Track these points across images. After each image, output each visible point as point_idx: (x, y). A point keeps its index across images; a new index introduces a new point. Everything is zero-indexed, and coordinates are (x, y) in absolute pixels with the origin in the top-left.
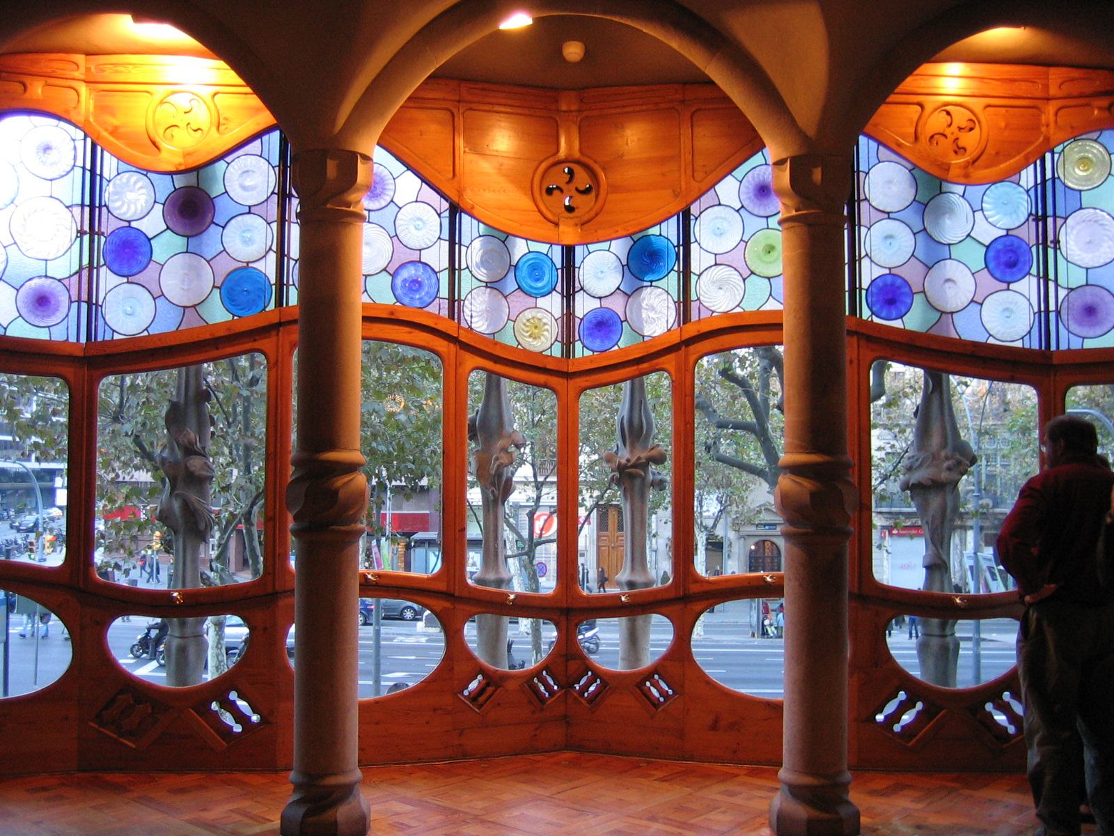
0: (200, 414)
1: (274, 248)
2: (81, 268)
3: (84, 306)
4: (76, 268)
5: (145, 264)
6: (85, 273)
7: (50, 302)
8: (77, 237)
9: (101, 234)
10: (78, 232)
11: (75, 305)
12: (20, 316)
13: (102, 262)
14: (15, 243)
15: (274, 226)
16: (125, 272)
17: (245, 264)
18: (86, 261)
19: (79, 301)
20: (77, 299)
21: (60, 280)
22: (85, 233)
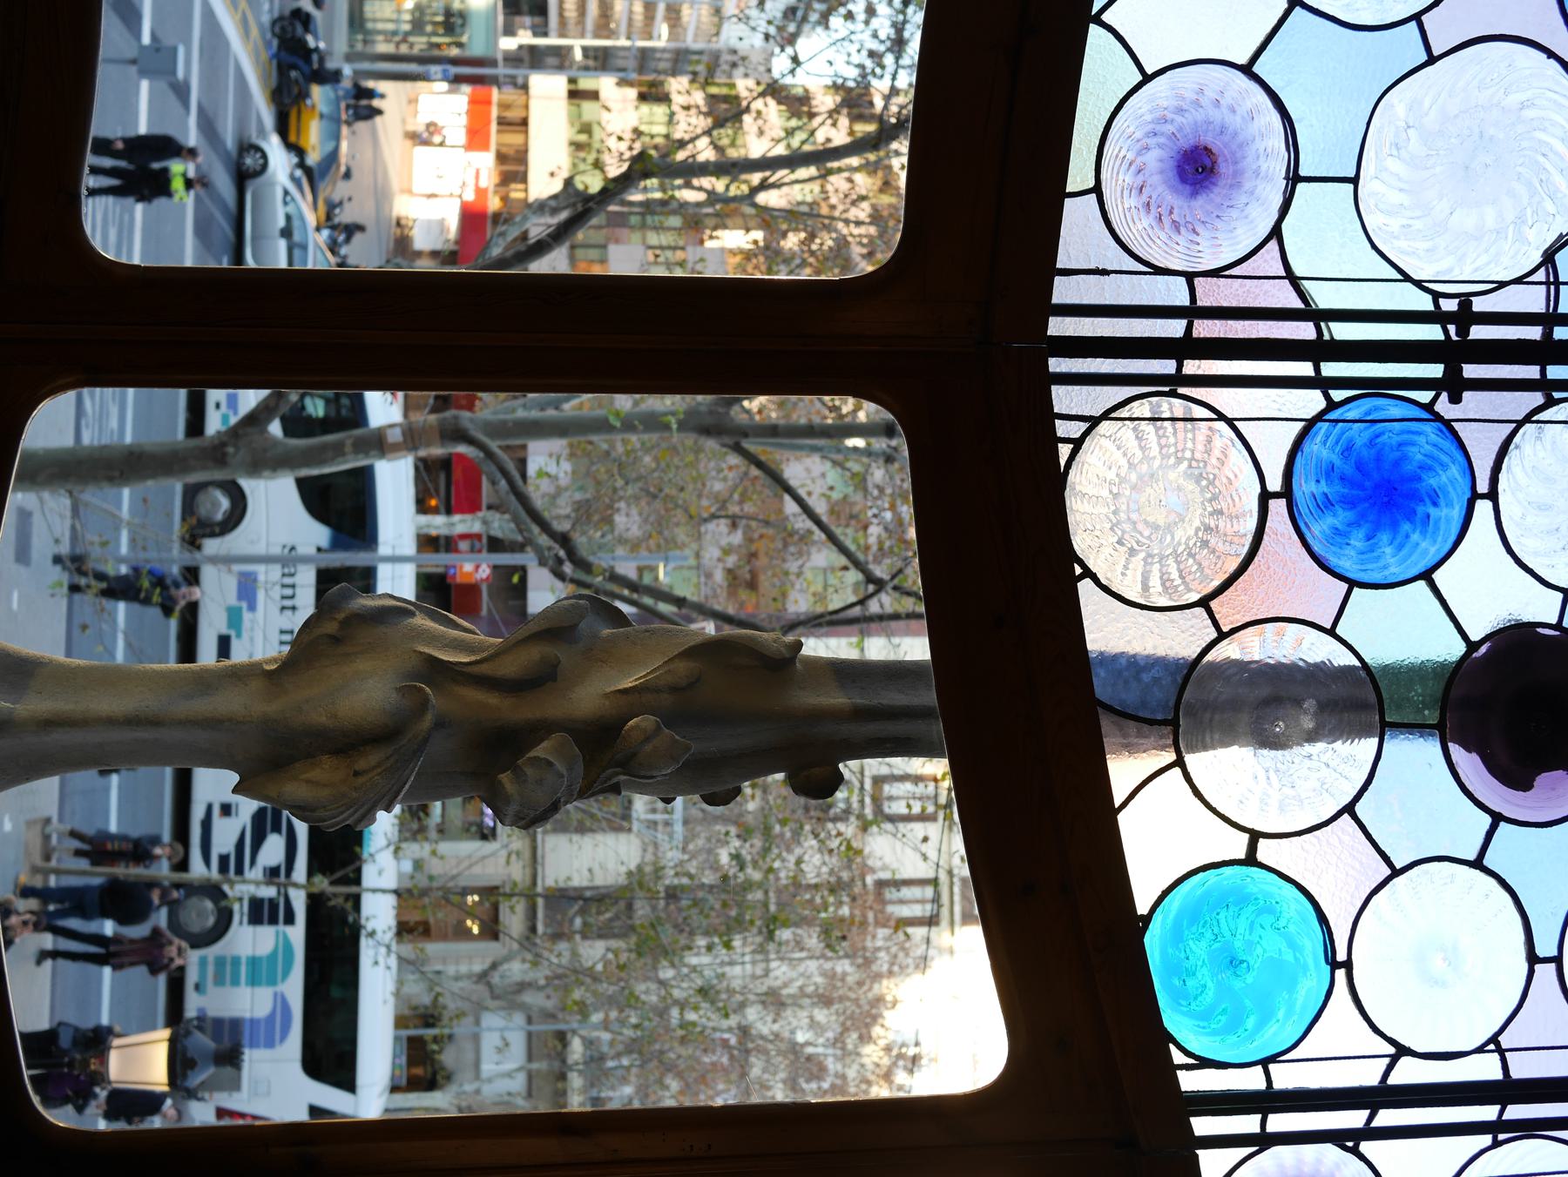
0: (756, 763)
1: (1409, 1073)
2: (1321, 316)
3: (1174, 328)
4: (1325, 297)
5: (1333, 561)
6: (1304, 331)
7: (1194, 194)
8: (1436, 296)
9: (1454, 386)
10: (1465, 300)
11: (1174, 293)
12: (1147, 78)
13: (1338, 395)
14: (1432, 60)
15: (1486, 1069)
16: (1305, 487)
17: (1341, 956)
18: (1343, 331)
19: (1192, 312)
20: (1202, 301)
21: (1276, 233)
22: (1463, 331)
